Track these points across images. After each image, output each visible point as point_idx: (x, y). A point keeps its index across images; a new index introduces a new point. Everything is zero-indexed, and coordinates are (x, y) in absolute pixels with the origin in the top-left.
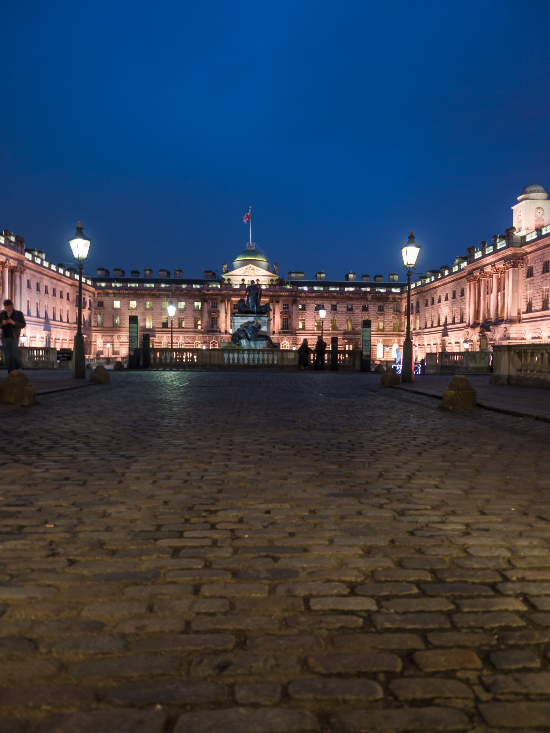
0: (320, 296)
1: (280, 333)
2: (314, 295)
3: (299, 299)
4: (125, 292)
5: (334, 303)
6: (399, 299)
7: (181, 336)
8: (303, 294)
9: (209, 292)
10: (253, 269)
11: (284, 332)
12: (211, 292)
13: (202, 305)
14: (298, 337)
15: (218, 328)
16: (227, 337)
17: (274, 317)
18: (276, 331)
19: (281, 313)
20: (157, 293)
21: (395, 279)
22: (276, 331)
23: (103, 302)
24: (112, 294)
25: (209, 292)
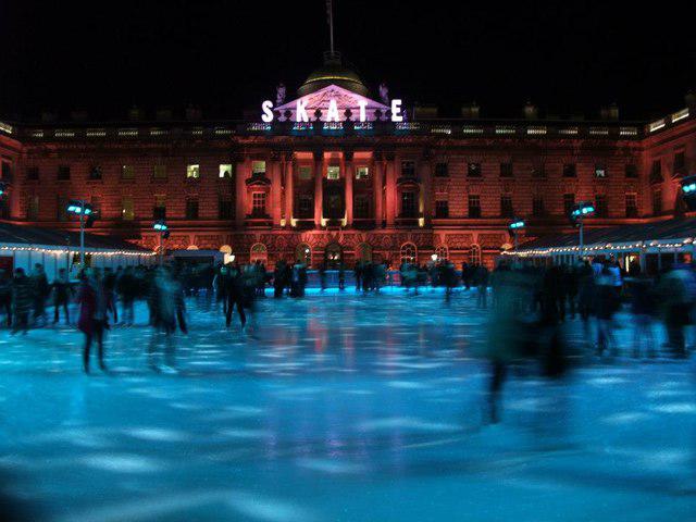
0: (476, 145)
1: (397, 223)
2: (464, 142)
3: (434, 151)
4: (80, 147)
5: (507, 160)
6: (635, 149)
7: (192, 236)
8: (442, 142)
9: (246, 141)
10: (338, 95)
11: (404, 223)
12: (251, 139)
13: (234, 170)
14: (435, 232)
15: (268, 217)
16: (285, 235)
17: (384, 192)
18: (390, 220)
19: (399, 181)
20: (144, 146)
21: (613, 115)
22: (390, 220)
23: (38, 169)
24: (55, 151)
25: (246, 141)
